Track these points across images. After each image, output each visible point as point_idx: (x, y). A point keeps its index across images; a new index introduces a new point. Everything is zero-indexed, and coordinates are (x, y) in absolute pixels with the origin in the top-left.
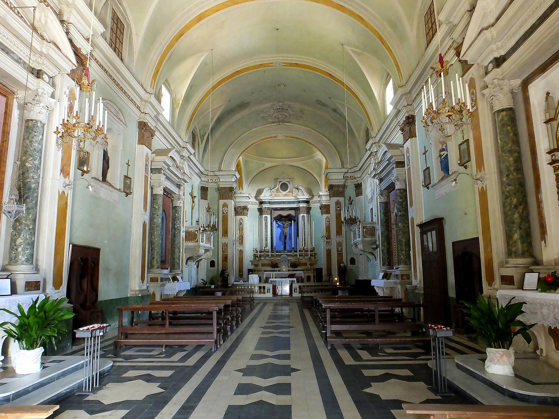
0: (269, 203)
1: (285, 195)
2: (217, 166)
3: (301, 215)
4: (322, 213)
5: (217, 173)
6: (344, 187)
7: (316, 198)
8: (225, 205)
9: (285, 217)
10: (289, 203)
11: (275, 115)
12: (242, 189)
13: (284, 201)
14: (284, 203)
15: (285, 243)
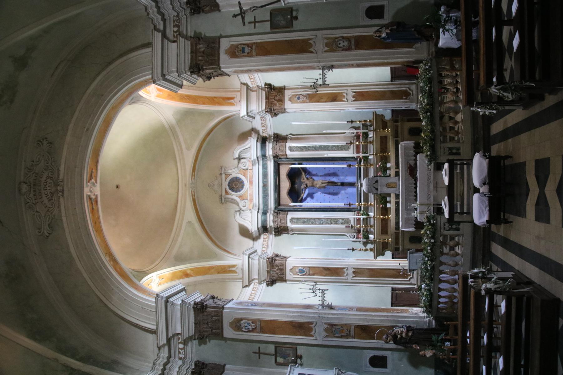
0: (265, 213)
1: (251, 183)
2: (151, 337)
3: (288, 152)
4: (283, 111)
5: (163, 340)
6: (197, 39)
7: (257, 124)
8: (237, 324)
9: (293, 183)
10: (265, 175)
11: (46, 201)
12: (234, 266)
13: (261, 185)
14: (265, 186)
15: (343, 184)
